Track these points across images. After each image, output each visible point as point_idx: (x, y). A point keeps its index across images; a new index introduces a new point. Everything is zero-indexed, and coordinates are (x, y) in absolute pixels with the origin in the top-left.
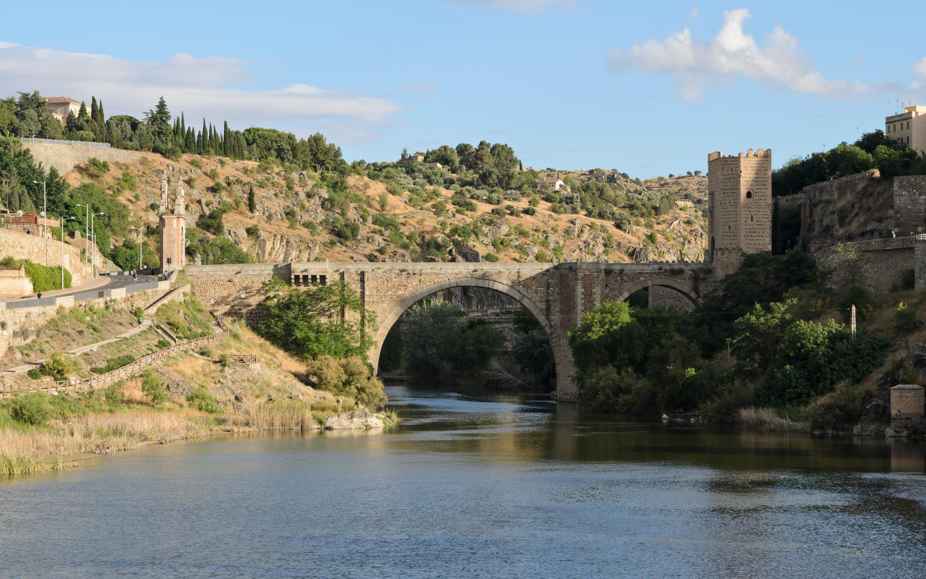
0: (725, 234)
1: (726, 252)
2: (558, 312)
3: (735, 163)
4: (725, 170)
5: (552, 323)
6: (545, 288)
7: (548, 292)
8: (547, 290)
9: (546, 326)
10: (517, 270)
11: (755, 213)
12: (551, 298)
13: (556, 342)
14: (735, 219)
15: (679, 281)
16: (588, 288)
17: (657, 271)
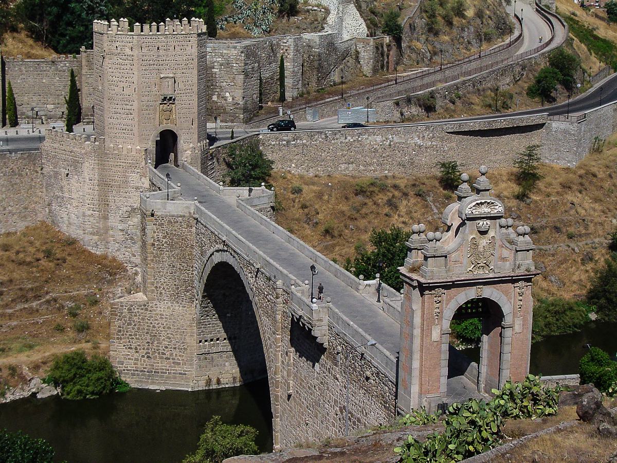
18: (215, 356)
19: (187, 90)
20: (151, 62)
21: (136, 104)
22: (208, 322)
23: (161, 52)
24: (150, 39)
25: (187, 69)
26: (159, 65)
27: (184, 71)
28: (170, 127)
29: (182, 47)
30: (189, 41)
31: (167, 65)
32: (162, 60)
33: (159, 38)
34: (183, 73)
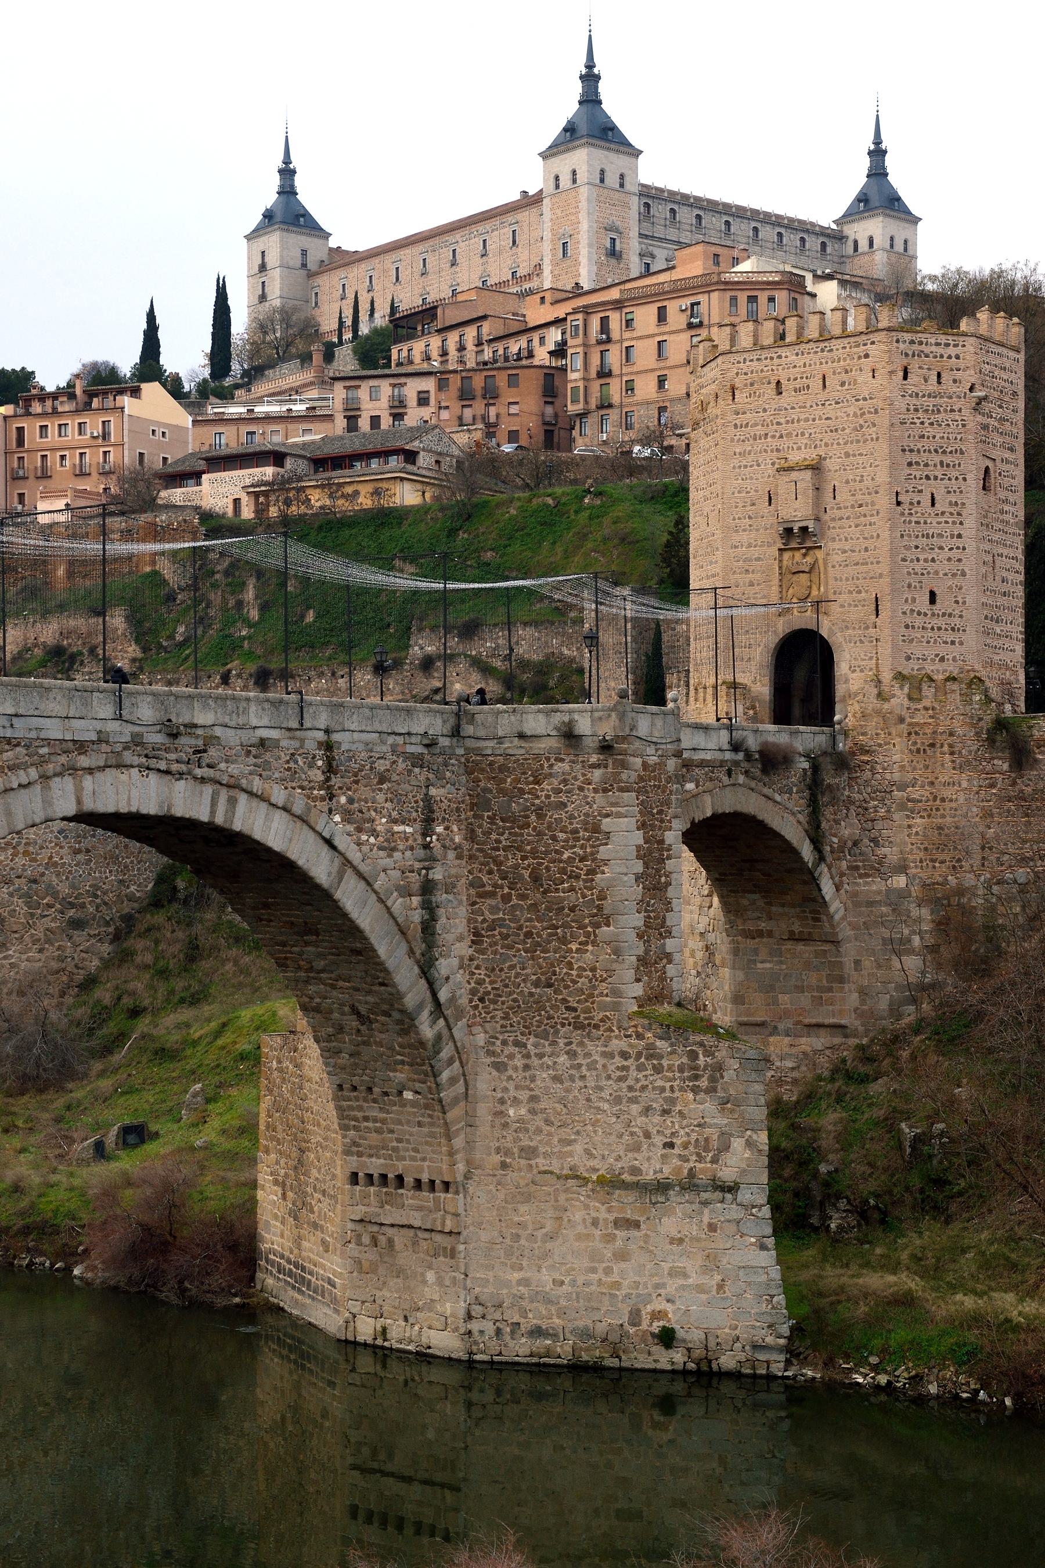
0: (919, 621)
1: (928, 691)
2: (460, 939)
3: (952, 351)
4: (912, 378)
5: (443, 995)
6: (418, 826)
7: (426, 846)
8: (424, 835)
9: (420, 1006)
10: (320, 736)
11: (1000, 551)
12: (437, 874)
13: (453, 1081)
14: (954, 566)
15: (778, 798)
16: (653, 826)
17: (728, 756)
18: (400, 1238)
19: (861, 506)
20: (759, 430)
21: (719, 554)
22: (360, 1108)
23: (787, 398)
24: (755, 363)
25: (858, 441)
26: (781, 437)
27: (849, 448)
28: (801, 618)
29: (844, 377)
30: (867, 356)
31: (803, 434)
32: (787, 422)
33: (780, 357)
34: (847, 455)
